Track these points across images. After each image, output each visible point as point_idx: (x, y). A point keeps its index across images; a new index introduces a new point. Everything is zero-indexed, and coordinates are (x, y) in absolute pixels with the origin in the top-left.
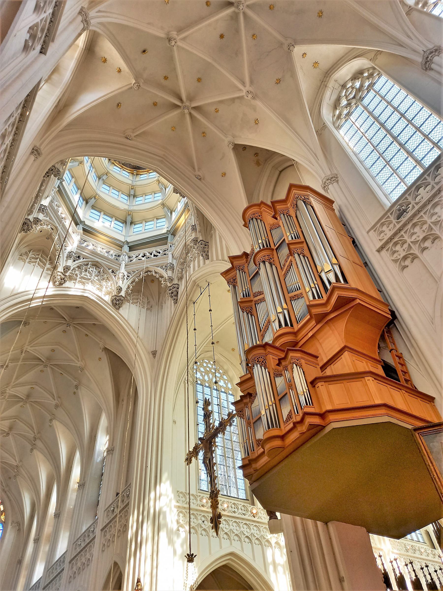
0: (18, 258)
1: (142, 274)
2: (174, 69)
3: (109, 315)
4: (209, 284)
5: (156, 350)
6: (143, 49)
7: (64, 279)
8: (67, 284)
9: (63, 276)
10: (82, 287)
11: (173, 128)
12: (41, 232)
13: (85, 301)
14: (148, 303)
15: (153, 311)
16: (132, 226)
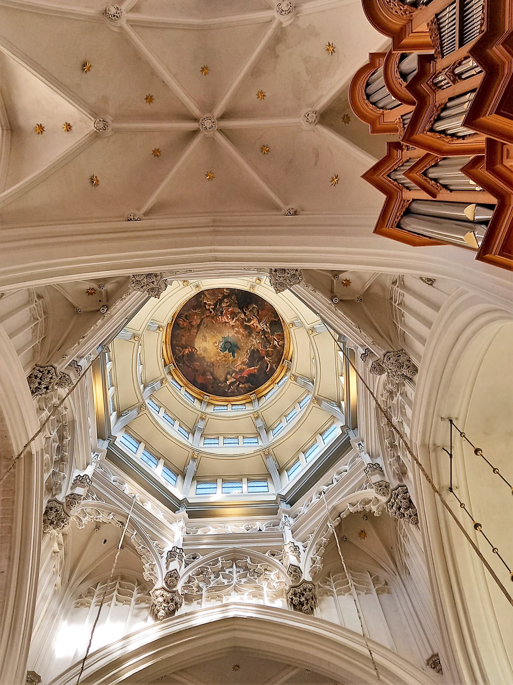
0: (73, 606)
1: (329, 525)
2: (153, 73)
3: (296, 634)
4: (451, 421)
5: (436, 652)
6: (79, 64)
7: (172, 600)
8: (184, 609)
9: (168, 595)
10: (215, 603)
11: (210, 176)
12: (105, 542)
13: (234, 630)
14: (376, 580)
15: (392, 591)
16: (282, 474)
